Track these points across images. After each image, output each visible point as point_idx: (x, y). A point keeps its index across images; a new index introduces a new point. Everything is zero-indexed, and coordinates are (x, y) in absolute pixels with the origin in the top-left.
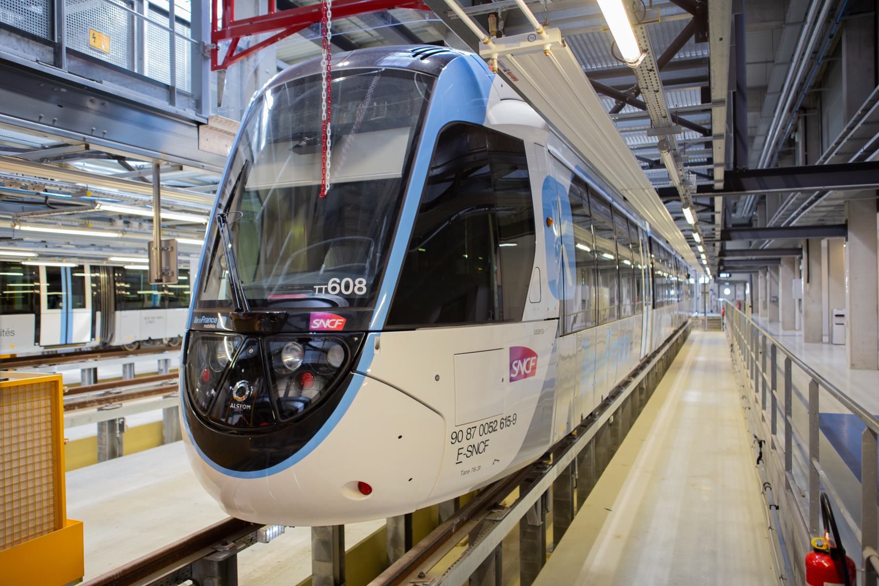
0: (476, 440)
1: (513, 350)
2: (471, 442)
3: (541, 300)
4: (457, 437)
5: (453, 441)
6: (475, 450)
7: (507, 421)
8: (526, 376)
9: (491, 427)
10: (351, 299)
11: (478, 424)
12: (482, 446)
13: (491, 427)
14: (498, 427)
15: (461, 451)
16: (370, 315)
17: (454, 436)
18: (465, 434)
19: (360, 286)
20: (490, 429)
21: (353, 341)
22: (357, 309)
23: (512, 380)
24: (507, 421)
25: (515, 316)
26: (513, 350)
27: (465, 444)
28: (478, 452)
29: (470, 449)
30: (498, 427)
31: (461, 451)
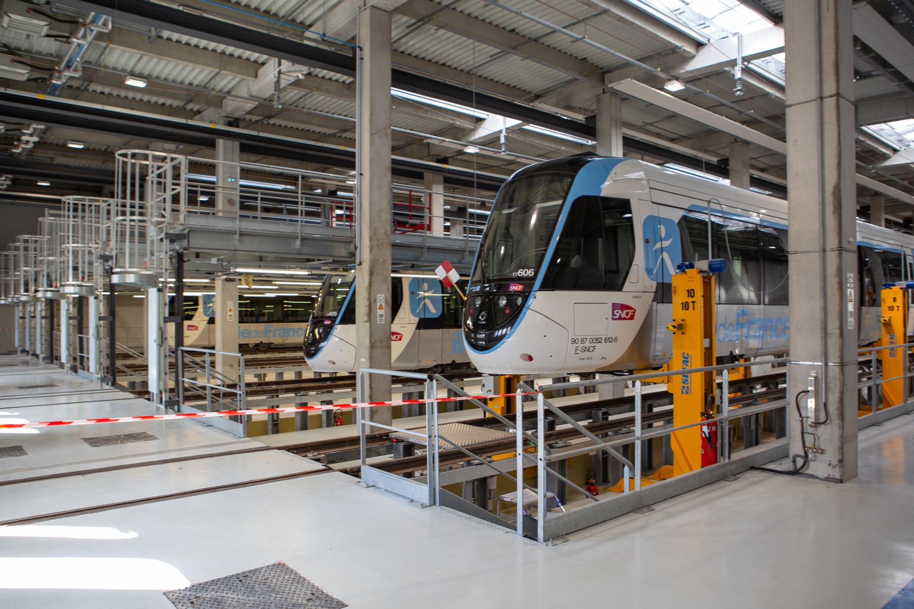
0: (587, 344)
1: (613, 304)
2: (584, 345)
3: (639, 282)
6: (585, 349)
7: (609, 340)
8: (625, 319)
9: (598, 341)
10: (528, 278)
12: (591, 349)
13: (598, 341)
16: (533, 284)
19: (530, 273)
21: (526, 295)
22: (528, 283)
23: (613, 319)
24: (609, 340)
25: (618, 287)
26: (613, 304)
27: (580, 345)
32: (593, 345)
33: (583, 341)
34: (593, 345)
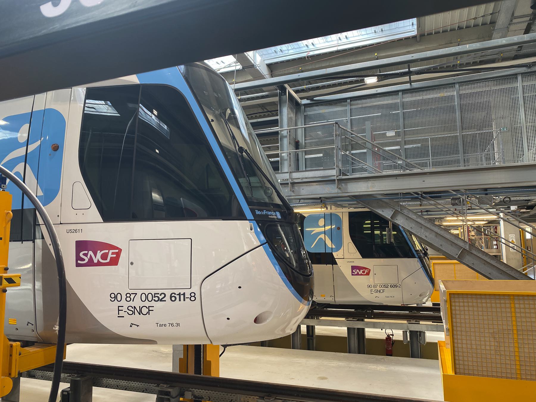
0: (137, 303)
2: (131, 303)
4: (116, 297)
5: (113, 300)
6: (133, 311)
11: (139, 293)
12: (145, 310)
14: (167, 298)
15: (120, 308)
17: (113, 296)
18: (124, 297)
20: (156, 299)
28: (140, 313)
29: (130, 308)
30: (167, 298)
31: (120, 308)
32: (147, 304)
33: (129, 297)
34: (147, 304)
